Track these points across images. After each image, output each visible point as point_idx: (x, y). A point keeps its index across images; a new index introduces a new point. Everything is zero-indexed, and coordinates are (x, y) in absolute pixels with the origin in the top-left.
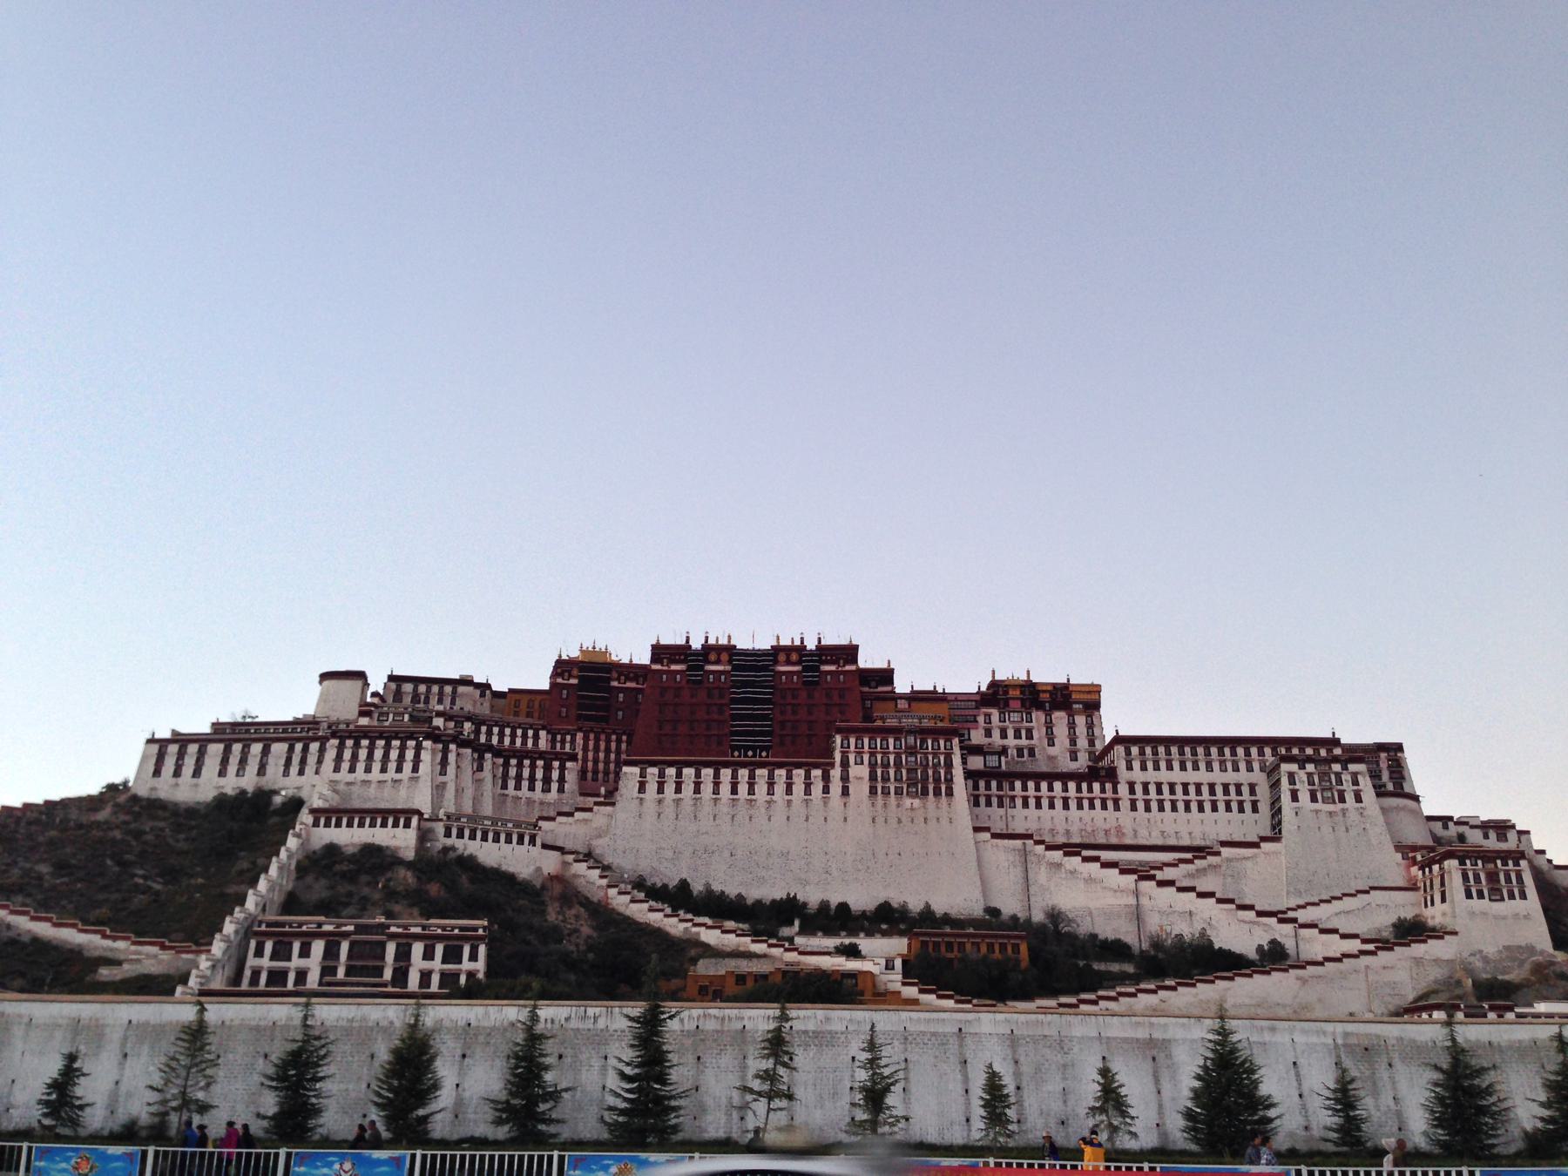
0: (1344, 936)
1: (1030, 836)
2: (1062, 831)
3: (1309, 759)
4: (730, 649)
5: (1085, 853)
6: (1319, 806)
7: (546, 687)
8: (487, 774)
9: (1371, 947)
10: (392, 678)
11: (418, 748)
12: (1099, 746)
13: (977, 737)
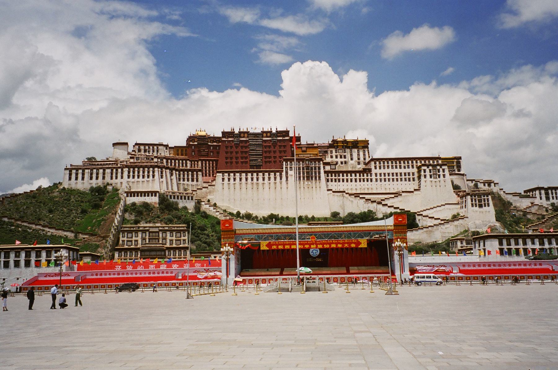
0: (436, 219)
1: (344, 192)
2: (354, 189)
3: (430, 165)
4: (247, 133)
5: (361, 196)
6: (432, 179)
7: (185, 145)
8: (174, 177)
9: (443, 222)
10: (136, 144)
11: (153, 172)
12: (368, 160)
13: (328, 160)
